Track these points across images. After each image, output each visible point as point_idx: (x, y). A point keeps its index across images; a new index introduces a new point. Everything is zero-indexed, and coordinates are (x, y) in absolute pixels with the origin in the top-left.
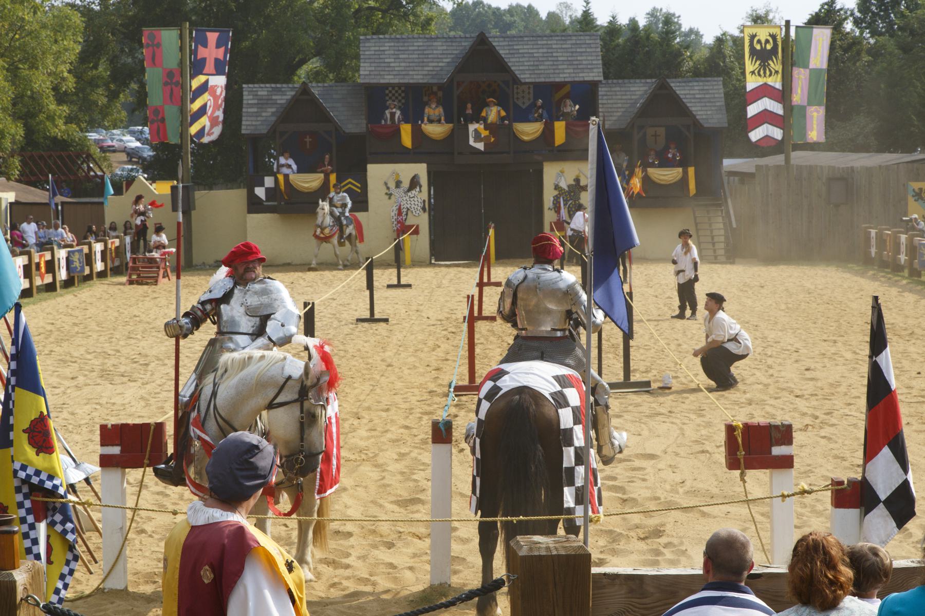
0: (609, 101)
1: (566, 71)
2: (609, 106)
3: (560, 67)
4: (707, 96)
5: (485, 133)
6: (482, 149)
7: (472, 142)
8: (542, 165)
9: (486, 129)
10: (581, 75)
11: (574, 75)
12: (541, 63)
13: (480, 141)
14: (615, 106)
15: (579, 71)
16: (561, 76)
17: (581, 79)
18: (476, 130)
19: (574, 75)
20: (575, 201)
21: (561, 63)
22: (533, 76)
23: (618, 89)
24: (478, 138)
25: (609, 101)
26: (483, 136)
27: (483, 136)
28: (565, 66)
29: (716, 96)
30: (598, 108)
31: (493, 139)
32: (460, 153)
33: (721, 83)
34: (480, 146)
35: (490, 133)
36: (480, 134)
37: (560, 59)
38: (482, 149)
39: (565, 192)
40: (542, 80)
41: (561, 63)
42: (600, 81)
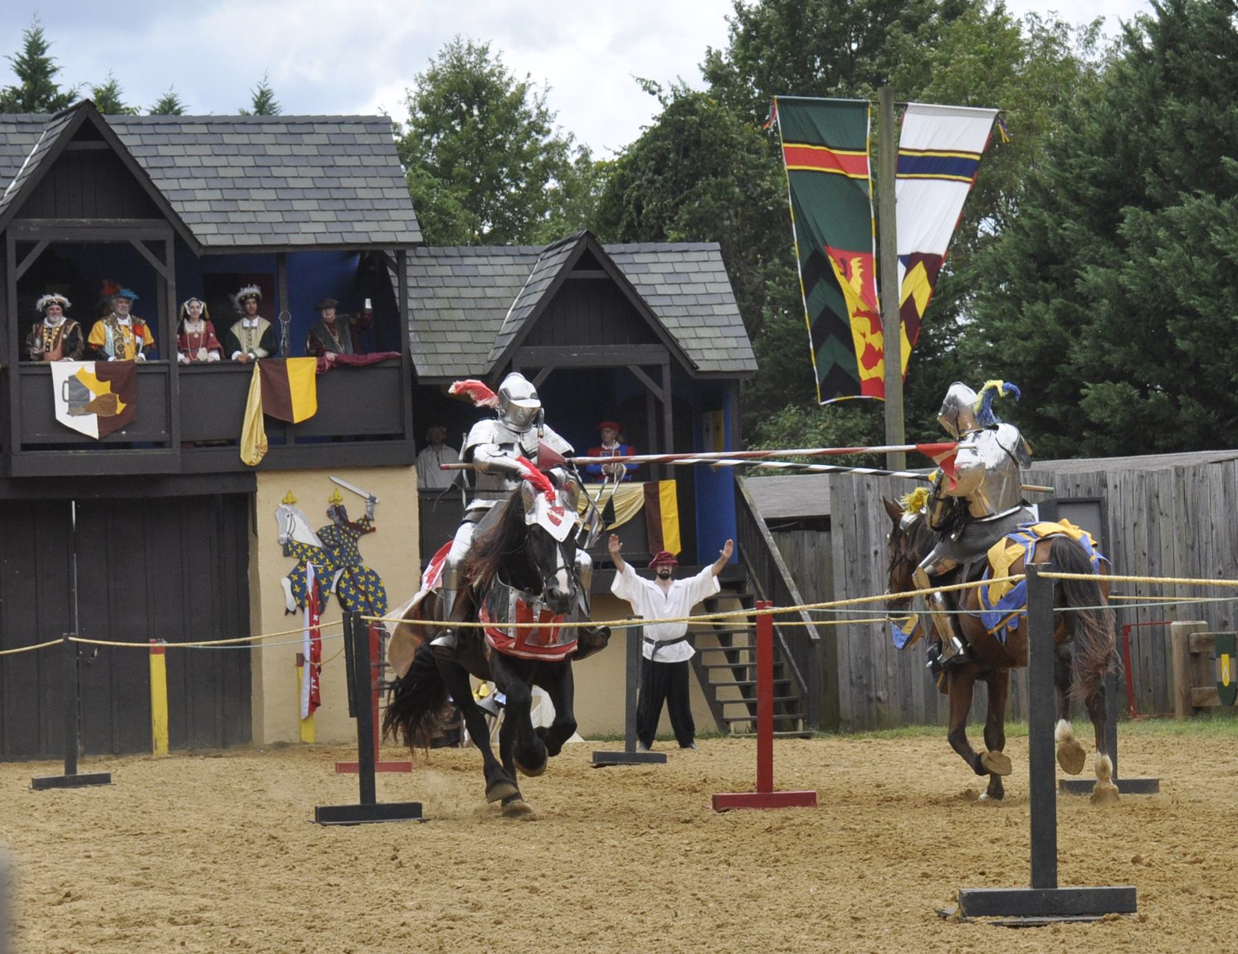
0: (429, 304)
1: (315, 216)
2: (432, 315)
3: (297, 205)
4: (687, 289)
5: (97, 389)
6: (96, 435)
7: (62, 413)
8: (255, 479)
9: (101, 375)
10: (358, 227)
11: (341, 228)
12: (242, 194)
13: (88, 410)
15: (353, 216)
16: (305, 228)
18: (73, 381)
19: (341, 228)
20: (349, 569)
21: (299, 194)
22: (225, 229)
23: (447, 271)
24: (79, 403)
26: (93, 397)
27: (93, 397)
28: (312, 205)
29: (712, 288)
30: (407, 321)
31: (121, 407)
32: (26, 447)
33: (718, 256)
34: (88, 425)
35: (112, 389)
36: (88, 392)
37: (293, 183)
38: (96, 435)
40: (255, 240)
41: (299, 194)
42: (414, 245)
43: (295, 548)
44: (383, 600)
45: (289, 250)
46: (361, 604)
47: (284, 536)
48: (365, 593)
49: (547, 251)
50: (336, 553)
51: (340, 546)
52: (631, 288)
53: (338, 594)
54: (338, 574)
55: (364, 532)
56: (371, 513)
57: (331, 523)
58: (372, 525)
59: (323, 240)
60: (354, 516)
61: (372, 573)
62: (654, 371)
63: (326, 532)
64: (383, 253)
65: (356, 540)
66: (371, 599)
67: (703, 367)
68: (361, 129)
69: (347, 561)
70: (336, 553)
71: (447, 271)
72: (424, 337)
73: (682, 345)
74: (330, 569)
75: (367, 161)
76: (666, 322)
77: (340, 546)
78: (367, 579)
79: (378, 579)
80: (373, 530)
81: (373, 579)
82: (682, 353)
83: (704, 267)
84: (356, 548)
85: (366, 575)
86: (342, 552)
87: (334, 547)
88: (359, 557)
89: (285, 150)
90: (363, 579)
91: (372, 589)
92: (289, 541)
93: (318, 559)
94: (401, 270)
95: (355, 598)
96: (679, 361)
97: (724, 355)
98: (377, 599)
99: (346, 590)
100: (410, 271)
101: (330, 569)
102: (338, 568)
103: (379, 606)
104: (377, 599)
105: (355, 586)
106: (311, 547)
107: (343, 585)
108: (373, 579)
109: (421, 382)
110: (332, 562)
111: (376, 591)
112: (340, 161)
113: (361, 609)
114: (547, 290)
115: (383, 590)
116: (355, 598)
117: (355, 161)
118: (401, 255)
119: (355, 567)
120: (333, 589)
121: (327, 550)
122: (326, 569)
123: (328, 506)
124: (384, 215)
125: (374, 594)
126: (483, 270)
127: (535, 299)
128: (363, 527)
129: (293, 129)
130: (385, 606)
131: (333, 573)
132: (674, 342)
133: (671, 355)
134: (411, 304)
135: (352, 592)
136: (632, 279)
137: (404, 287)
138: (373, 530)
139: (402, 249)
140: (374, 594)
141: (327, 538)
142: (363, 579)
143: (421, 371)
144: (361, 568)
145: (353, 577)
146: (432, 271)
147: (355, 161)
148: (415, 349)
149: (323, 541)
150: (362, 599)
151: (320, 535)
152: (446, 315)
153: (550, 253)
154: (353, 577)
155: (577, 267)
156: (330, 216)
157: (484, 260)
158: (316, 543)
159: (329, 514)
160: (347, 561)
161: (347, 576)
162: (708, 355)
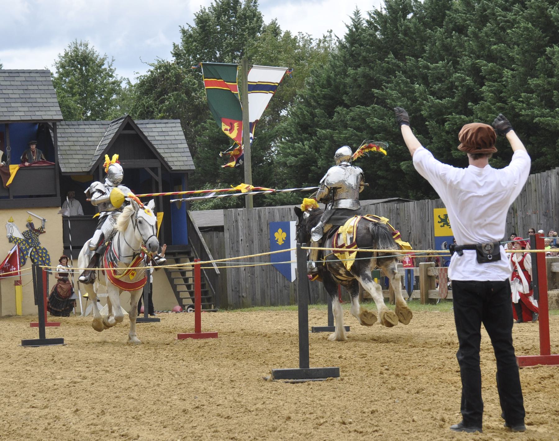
0: (66, 144)
1: (20, 109)
2: (67, 148)
4: (167, 138)
10: (37, 113)
14: (72, 148)
16: (16, 114)
17: (40, 118)
20: (36, 248)
21: (14, 100)
23: (73, 131)
25: (66, 144)
29: (177, 138)
33: (180, 125)
39: (22, 242)
41: (14, 100)
42: (60, 120)
43: (13, 239)
44: (49, 259)
45: (10, 122)
46: (40, 261)
47: (9, 235)
48: (41, 257)
49: (112, 123)
50: (30, 241)
51: (31, 238)
52: (146, 137)
53: (31, 257)
54: (31, 249)
55: (41, 233)
56: (44, 225)
57: (28, 229)
58: (44, 230)
59: (23, 118)
60: (37, 227)
61: (44, 249)
62: (154, 169)
63: (26, 233)
64: (47, 124)
65: (38, 236)
66: (44, 259)
67: (174, 168)
68: (38, 75)
69: (34, 244)
70: (30, 241)
71: (73, 131)
72: (64, 157)
73: (166, 159)
74: (28, 247)
75: (40, 87)
76: (158, 150)
77: (31, 238)
78: (42, 251)
79: (47, 251)
80: (45, 232)
81: (45, 251)
82: (166, 163)
83: (174, 129)
84: (38, 240)
85: (42, 250)
86: (32, 241)
87: (29, 239)
88: (39, 243)
89: (8, 83)
90: (41, 251)
91: (44, 255)
92: (11, 237)
93: (23, 244)
94: (54, 130)
95: (37, 259)
96: (165, 166)
97: (182, 163)
98: (46, 259)
99: (34, 256)
100: (58, 131)
101: (28, 247)
102: (31, 247)
103: (47, 262)
104: (46, 259)
105: (38, 254)
106: (20, 239)
107: (33, 254)
108: (45, 251)
109: (63, 174)
110: (28, 245)
111: (46, 256)
112: (30, 87)
113: (40, 263)
114: (113, 138)
115: (48, 255)
116: (37, 259)
117: (36, 87)
118: (55, 124)
119: (38, 246)
120: (29, 255)
121: (26, 240)
122: (26, 247)
123: (26, 223)
124: (48, 109)
125: (45, 257)
126: (87, 130)
127: (107, 142)
128: (41, 231)
129: (11, 75)
130: (50, 262)
131: (29, 249)
132: (163, 158)
133: (162, 164)
134: (59, 144)
135: (36, 256)
136: (146, 134)
137: (56, 137)
138: (45, 232)
139: (55, 122)
140: (45, 257)
141: (26, 235)
142: (41, 251)
143: (63, 170)
144: (40, 247)
145: (37, 251)
146: (67, 131)
147: (36, 87)
148: (61, 161)
149: (25, 236)
150: (40, 259)
151: (23, 234)
152: (72, 148)
153: (114, 124)
154: (37, 251)
155: (125, 129)
156: (26, 109)
157: (87, 127)
158: (22, 237)
159: (27, 226)
160: (34, 244)
161: (34, 250)
162: (176, 163)
